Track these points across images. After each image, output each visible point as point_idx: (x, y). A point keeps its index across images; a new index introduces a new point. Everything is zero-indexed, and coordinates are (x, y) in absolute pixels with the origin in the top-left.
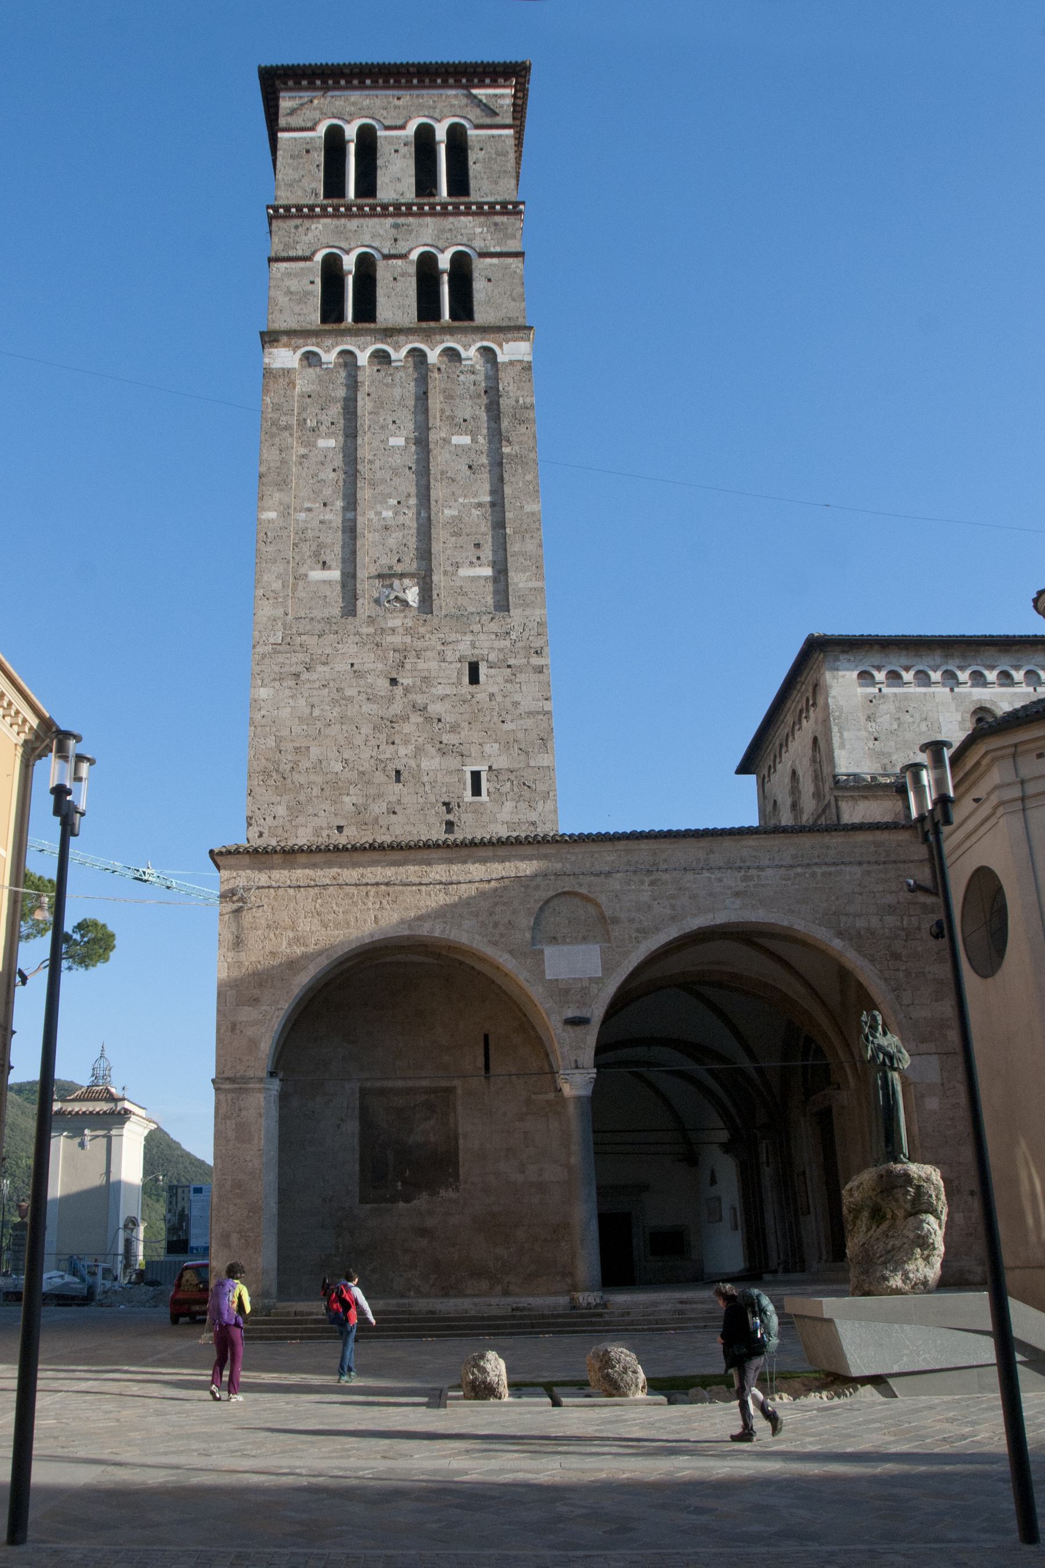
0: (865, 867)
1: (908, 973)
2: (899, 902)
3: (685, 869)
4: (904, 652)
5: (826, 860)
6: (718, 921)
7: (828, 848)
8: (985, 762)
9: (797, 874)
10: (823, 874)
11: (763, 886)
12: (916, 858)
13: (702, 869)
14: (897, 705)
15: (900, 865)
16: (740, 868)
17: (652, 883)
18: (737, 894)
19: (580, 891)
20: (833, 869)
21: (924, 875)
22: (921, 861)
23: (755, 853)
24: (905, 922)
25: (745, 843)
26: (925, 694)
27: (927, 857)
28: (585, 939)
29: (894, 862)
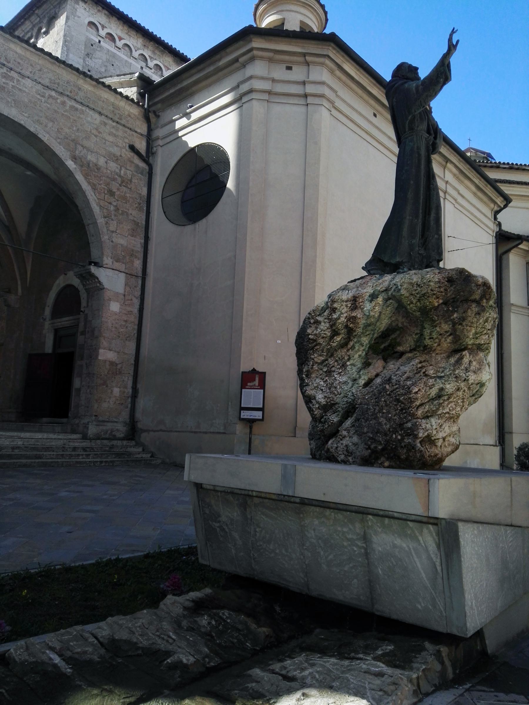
0: (103, 118)
1: (117, 209)
2: (121, 156)
4: (121, 27)
5: (76, 97)
7: (80, 89)
8: (241, 60)
9: (50, 96)
10: (72, 107)
11: (20, 90)
12: (139, 131)
14: (108, 57)
15: (127, 129)
16: (4, 65)
21: (141, 146)
22: (142, 135)
23: (20, 61)
24: (122, 172)
25: (12, 46)
26: (126, 61)
27: (146, 134)
29: (124, 126)
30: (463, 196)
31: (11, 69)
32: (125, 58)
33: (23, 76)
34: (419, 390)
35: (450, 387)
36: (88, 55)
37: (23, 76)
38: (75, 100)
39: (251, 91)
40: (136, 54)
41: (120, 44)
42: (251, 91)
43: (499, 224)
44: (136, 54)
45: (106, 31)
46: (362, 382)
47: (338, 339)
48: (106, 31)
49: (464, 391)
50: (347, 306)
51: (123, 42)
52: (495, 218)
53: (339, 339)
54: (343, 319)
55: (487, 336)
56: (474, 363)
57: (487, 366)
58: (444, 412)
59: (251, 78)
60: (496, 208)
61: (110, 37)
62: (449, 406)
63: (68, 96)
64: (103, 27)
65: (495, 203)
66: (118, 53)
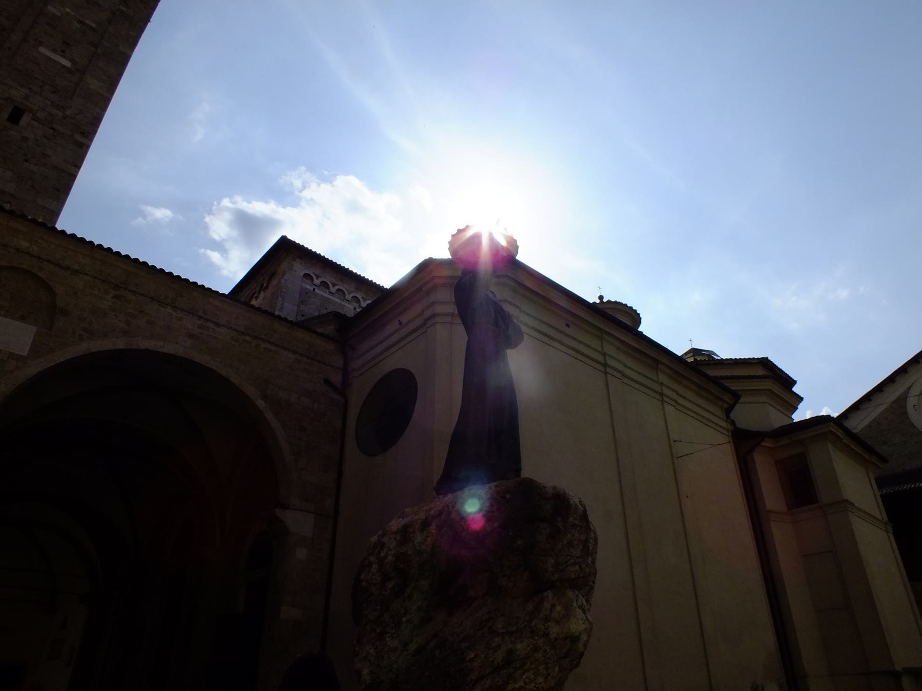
3: (152, 298)
6: (166, 350)
13: (168, 304)
16: (201, 317)
17: (114, 297)
18: (191, 336)
19: (40, 274)
20: (273, 348)
28: (23, 318)
30: (682, 396)
31: (208, 320)
32: (339, 301)
33: (218, 325)
34: (476, 656)
35: (521, 647)
36: (302, 302)
37: (218, 325)
38: (269, 342)
39: (434, 316)
40: (349, 297)
41: (333, 290)
42: (434, 316)
43: (733, 423)
44: (349, 297)
45: (321, 280)
46: (413, 647)
47: (390, 585)
48: (321, 280)
49: (545, 651)
50: (395, 539)
51: (337, 287)
52: (728, 417)
53: (390, 586)
54: (390, 558)
55: (577, 567)
56: (558, 608)
57: (580, 611)
58: (517, 686)
59: (433, 304)
60: (726, 406)
61: (324, 285)
62: (524, 677)
63: (262, 339)
64: (318, 277)
65: (724, 401)
66: (331, 297)
